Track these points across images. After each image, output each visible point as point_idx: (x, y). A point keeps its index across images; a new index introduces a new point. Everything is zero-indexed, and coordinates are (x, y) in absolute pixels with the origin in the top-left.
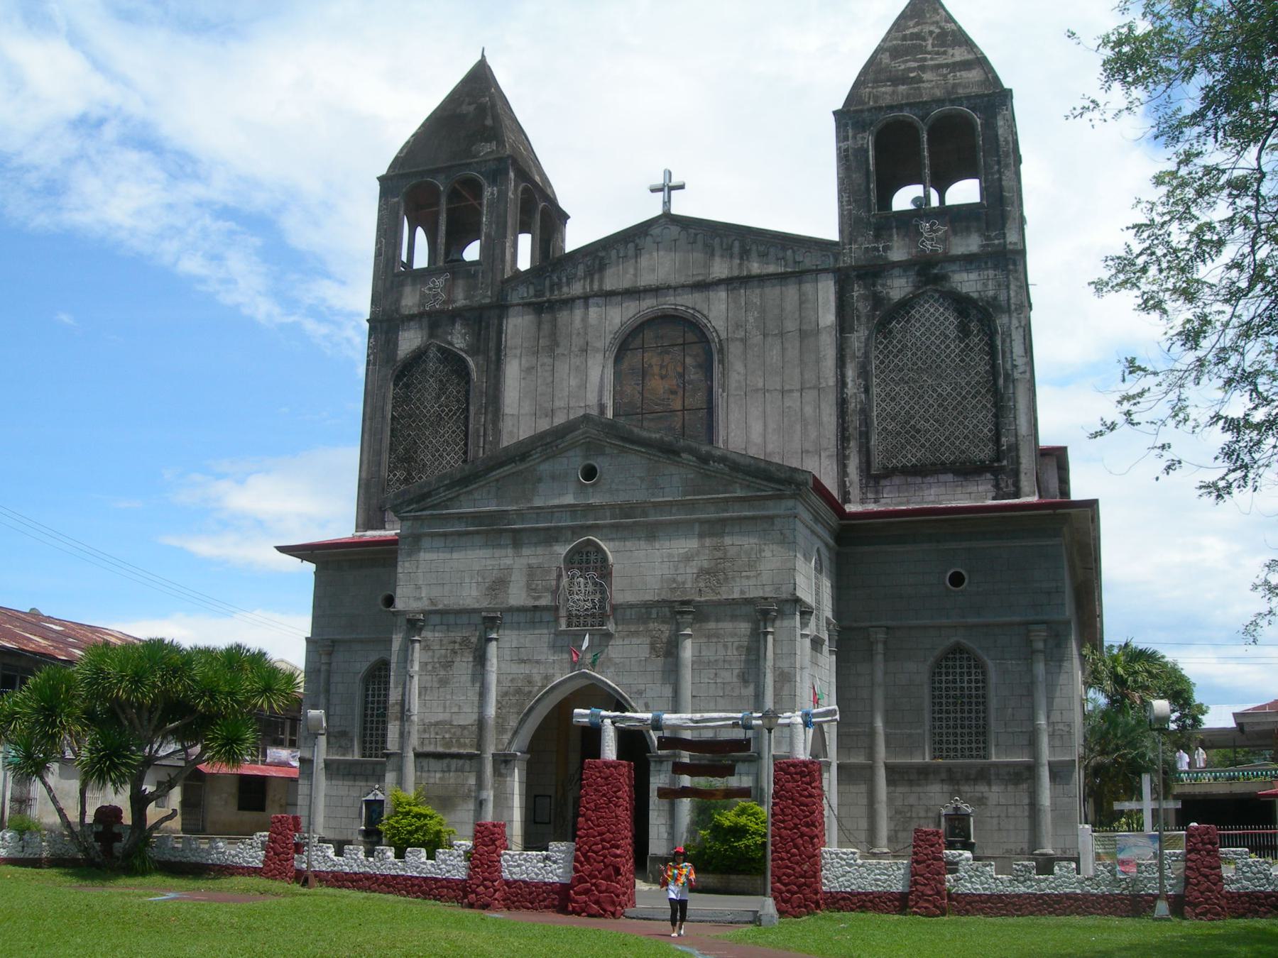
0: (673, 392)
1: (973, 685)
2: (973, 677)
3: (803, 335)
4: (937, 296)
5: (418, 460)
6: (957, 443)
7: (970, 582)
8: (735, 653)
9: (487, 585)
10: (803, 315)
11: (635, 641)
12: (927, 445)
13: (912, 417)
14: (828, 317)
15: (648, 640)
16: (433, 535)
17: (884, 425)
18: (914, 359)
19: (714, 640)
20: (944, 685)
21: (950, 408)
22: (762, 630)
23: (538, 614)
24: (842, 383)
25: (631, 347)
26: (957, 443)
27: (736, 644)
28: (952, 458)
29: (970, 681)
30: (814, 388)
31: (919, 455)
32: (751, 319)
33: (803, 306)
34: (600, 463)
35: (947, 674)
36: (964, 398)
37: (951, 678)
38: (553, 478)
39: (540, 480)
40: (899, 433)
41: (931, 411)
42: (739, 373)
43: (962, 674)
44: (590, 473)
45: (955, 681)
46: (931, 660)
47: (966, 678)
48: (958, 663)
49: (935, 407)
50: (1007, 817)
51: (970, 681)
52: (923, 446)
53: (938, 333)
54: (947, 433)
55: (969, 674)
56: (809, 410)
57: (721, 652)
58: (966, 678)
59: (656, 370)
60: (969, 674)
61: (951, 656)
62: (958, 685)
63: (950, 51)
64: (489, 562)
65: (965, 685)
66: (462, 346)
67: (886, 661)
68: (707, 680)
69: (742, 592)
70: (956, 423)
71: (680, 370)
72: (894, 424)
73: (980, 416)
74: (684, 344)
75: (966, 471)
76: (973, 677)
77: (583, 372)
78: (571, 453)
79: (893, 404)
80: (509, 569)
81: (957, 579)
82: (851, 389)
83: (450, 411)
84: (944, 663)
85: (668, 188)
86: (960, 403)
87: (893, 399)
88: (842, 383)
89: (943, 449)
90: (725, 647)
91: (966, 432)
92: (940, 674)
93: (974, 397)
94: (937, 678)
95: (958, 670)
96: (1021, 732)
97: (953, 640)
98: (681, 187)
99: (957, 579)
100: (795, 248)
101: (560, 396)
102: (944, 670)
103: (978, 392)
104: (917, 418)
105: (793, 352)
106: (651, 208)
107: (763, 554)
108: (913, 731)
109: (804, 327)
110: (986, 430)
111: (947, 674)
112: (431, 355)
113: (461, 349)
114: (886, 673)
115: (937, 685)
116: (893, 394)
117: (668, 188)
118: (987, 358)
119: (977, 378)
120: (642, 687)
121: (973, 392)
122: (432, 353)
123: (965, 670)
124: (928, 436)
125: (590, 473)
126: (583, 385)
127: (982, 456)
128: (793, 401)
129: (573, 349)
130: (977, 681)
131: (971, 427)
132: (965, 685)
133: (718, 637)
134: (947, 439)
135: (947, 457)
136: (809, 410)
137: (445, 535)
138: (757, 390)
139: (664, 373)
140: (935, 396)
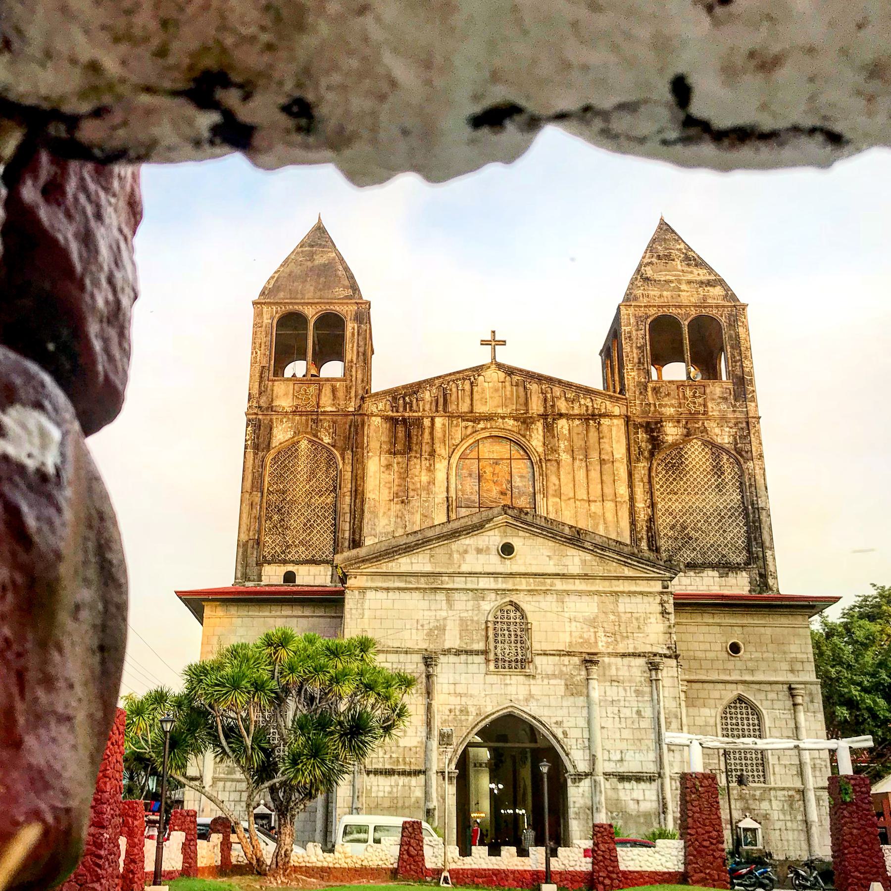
0: (503, 493)
1: (751, 727)
2: (751, 722)
3: (602, 462)
4: (700, 443)
5: (292, 528)
6: (720, 549)
7: (745, 651)
8: (634, 695)
9: (425, 632)
10: (601, 447)
11: (552, 682)
12: (698, 549)
13: (685, 528)
14: (620, 451)
15: (563, 682)
16: (376, 589)
17: (665, 532)
18: (685, 486)
19: (616, 684)
20: (729, 727)
21: (713, 524)
22: (654, 677)
23: (470, 658)
24: (632, 499)
25: (469, 457)
26: (720, 549)
27: (633, 689)
28: (717, 560)
29: (749, 725)
30: (612, 501)
31: (692, 556)
32: (562, 446)
33: (601, 441)
34: (516, 542)
35: (731, 718)
36: (723, 517)
37: (734, 721)
38: (479, 551)
39: (466, 552)
40: (676, 539)
41: (699, 525)
42: (555, 485)
43: (742, 719)
44: (507, 550)
45: (738, 725)
46: (720, 709)
47: (745, 722)
48: (738, 710)
49: (702, 522)
50: (786, 830)
51: (749, 725)
52: (694, 549)
53: (701, 470)
54: (712, 542)
55: (748, 719)
56: (610, 516)
57: (622, 693)
58: (745, 722)
59: (488, 475)
60: (748, 719)
61: (733, 705)
62: (740, 727)
63: (696, 272)
64: (426, 613)
65: (745, 727)
66: (330, 441)
67: (687, 707)
68: (612, 715)
69: (635, 648)
70: (718, 535)
71: (508, 477)
72: (672, 532)
73: (735, 531)
74: (510, 459)
75: (726, 567)
76: (751, 722)
77: (430, 470)
78: (491, 533)
79: (671, 518)
80: (445, 619)
81: (735, 648)
82: (640, 505)
83: (320, 491)
84: (728, 710)
85: (494, 342)
86: (720, 521)
87: (671, 514)
88: (632, 499)
89: (709, 553)
90: (625, 690)
91: (726, 542)
92: (726, 718)
93: (730, 517)
94: (724, 721)
95: (739, 716)
96: (791, 764)
97: (735, 693)
98: (504, 343)
99: (735, 648)
100: (593, 398)
101: (414, 488)
102: (728, 715)
103: (733, 514)
104: (689, 529)
105: (595, 474)
106: (483, 356)
107: (649, 621)
108: (711, 761)
109: (603, 457)
110: (740, 542)
111: (731, 718)
112: (303, 447)
113: (329, 444)
114: (687, 716)
115: (724, 727)
116: (670, 510)
117: (494, 342)
118: (738, 491)
119: (732, 504)
120: (560, 719)
121: (729, 514)
122: (304, 444)
123: (744, 716)
124: (698, 542)
125: (507, 550)
126: (432, 482)
127: (738, 560)
128: (595, 508)
129: (423, 453)
130: (754, 725)
131: (729, 539)
132: (745, 727)
133: (618, 682)
134: (712, 546)
135: (714, 559)
136: (610, 516)
137: (388, 589)
138: (569, 499)
139: (496, 479)
140: (702, 514)
